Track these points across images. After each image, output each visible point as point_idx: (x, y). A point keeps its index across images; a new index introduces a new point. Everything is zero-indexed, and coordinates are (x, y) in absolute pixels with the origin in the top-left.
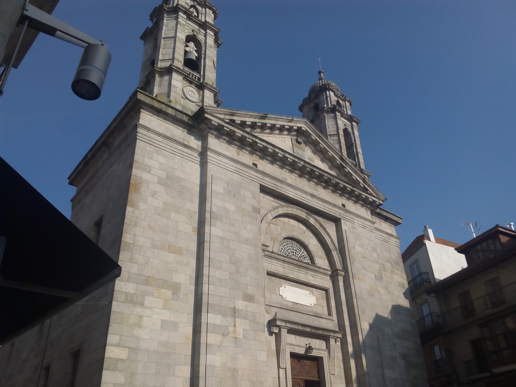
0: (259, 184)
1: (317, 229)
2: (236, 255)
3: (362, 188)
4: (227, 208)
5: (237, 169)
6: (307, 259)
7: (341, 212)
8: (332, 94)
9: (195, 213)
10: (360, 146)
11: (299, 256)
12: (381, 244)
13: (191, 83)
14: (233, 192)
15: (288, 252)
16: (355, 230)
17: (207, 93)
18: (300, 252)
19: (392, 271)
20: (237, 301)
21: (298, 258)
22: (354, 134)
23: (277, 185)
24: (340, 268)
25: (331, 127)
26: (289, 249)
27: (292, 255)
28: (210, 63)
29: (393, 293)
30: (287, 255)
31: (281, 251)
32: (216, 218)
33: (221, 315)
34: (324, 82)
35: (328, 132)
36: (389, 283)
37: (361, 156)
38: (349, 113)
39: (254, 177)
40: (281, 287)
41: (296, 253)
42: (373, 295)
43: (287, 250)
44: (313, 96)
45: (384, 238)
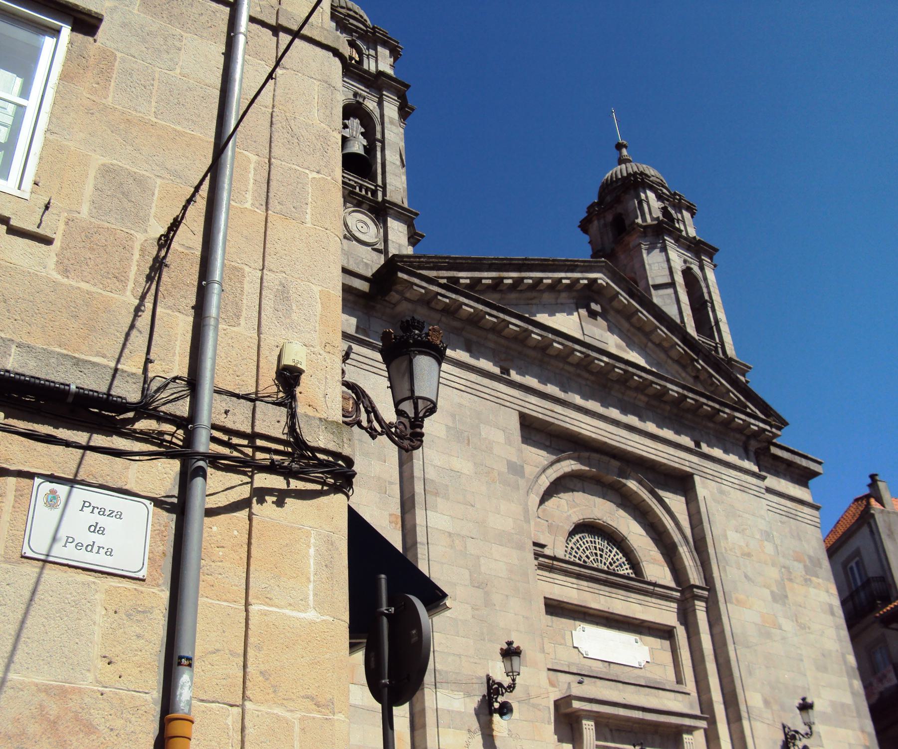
0: (517, 412)
1: (644, 500)
2: (483, 569)
3: (735, 403)
4: (456, 470)
5: (469, 384)
6: (626, 567)
7: (695, 459)
8: (651, 195)
9: (391, 483)
10: (721, 305)
11: (609, 562)
12: (781, 522)
14: (466, 434)
15: (585, 555)
16: (724, 497)
17: (392, 223)
18: (610, 551)
19: (806, 580)
20: (490, 663)
21: (608, 567)
22: (705, 279)
23: (555, 410)
24: (697, 583)
25: (655, 267)
26: (586, 547)
27: (594, 559)
28: (394, 157)
29: (809, 628)
30: (584, 561)
31: (570, 554)
32: (436, 493)
33: (460, 691)
34: (632, 168)
36: (800, 606)
37: (724, 328)
38: (692, 232)
39: (505, 397)
40: (576, 630)
41: (601, 556)
42: (768, 636)
43: (583, 550)
44: (608, 199)
45: (785, 509)
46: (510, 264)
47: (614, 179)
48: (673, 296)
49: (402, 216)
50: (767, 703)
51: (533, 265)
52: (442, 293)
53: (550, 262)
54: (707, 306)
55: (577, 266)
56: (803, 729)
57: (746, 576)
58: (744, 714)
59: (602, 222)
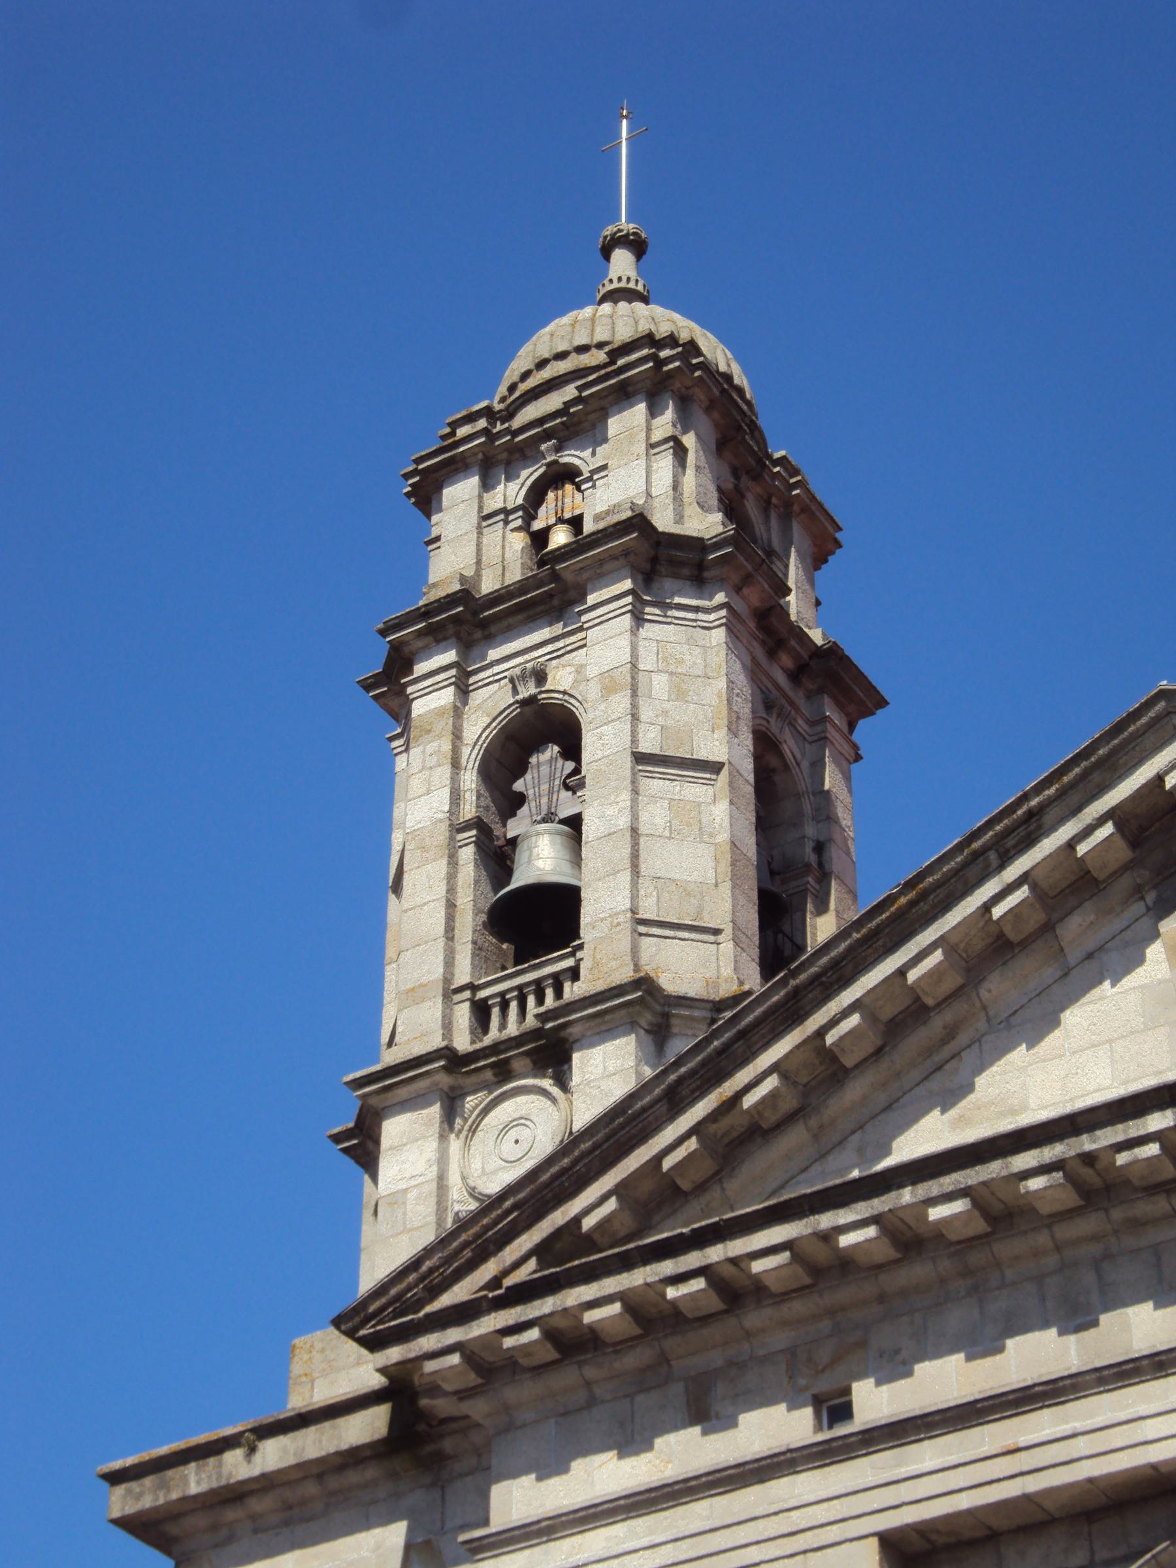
13: (504, 1072)
23: (1023, 1441)
39: (821, 1513)
46: (742, 1035)
49: (607, 1017)
51: (835, 964)
52: (511, 1322)
53: (903, 900)
55: (1031, 815)
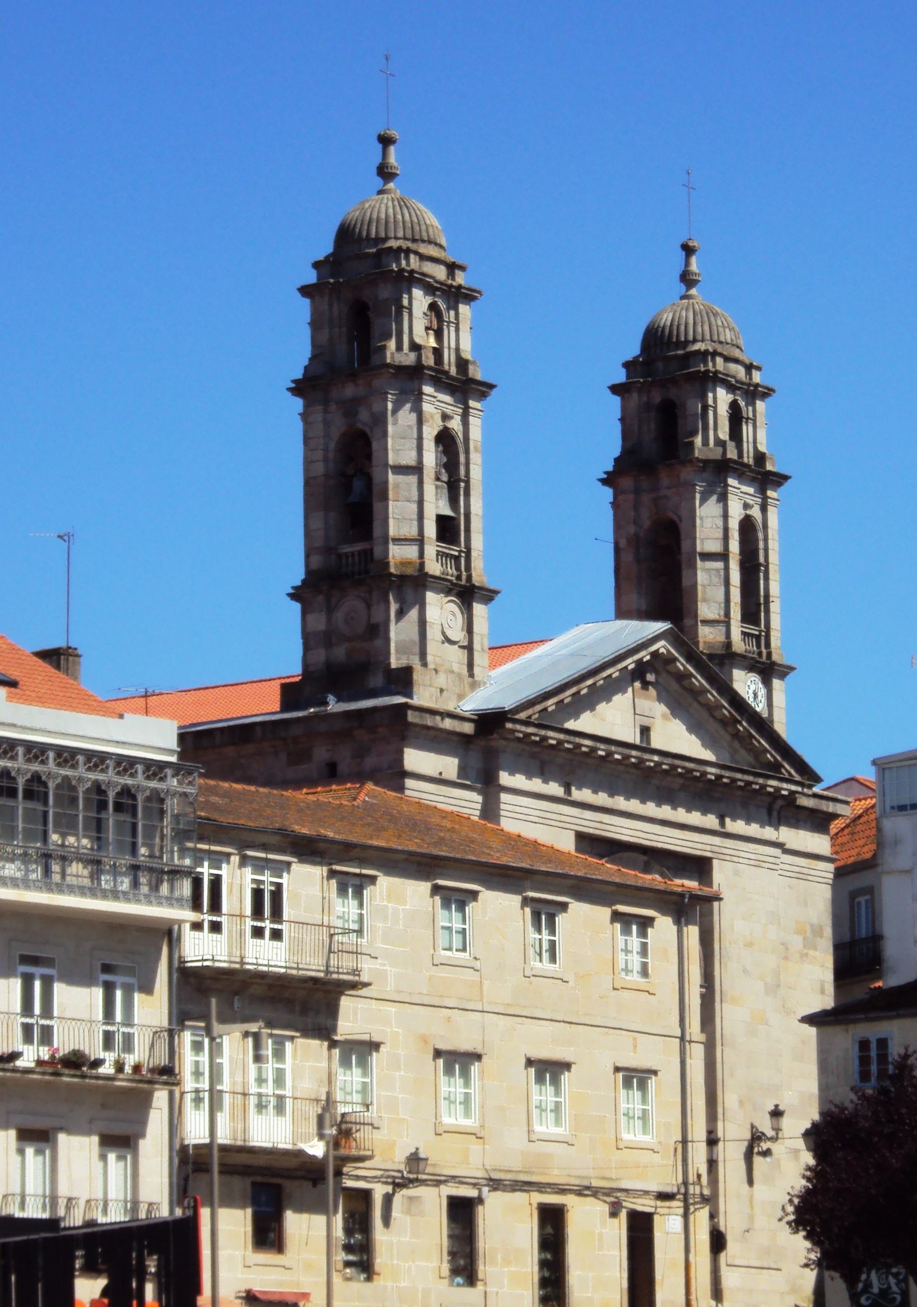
0: (573, 832)
22: (765, 526)
25: (708, 523)
35: (698, 542)
45: (797, 869)
47: (674, 340)
48: (722, 573)
50: (741, 1103)
54: (758, 571)
56: (770, 1133)
57: (745, 971)
58: (720, 1116)
59: (645, 399)
